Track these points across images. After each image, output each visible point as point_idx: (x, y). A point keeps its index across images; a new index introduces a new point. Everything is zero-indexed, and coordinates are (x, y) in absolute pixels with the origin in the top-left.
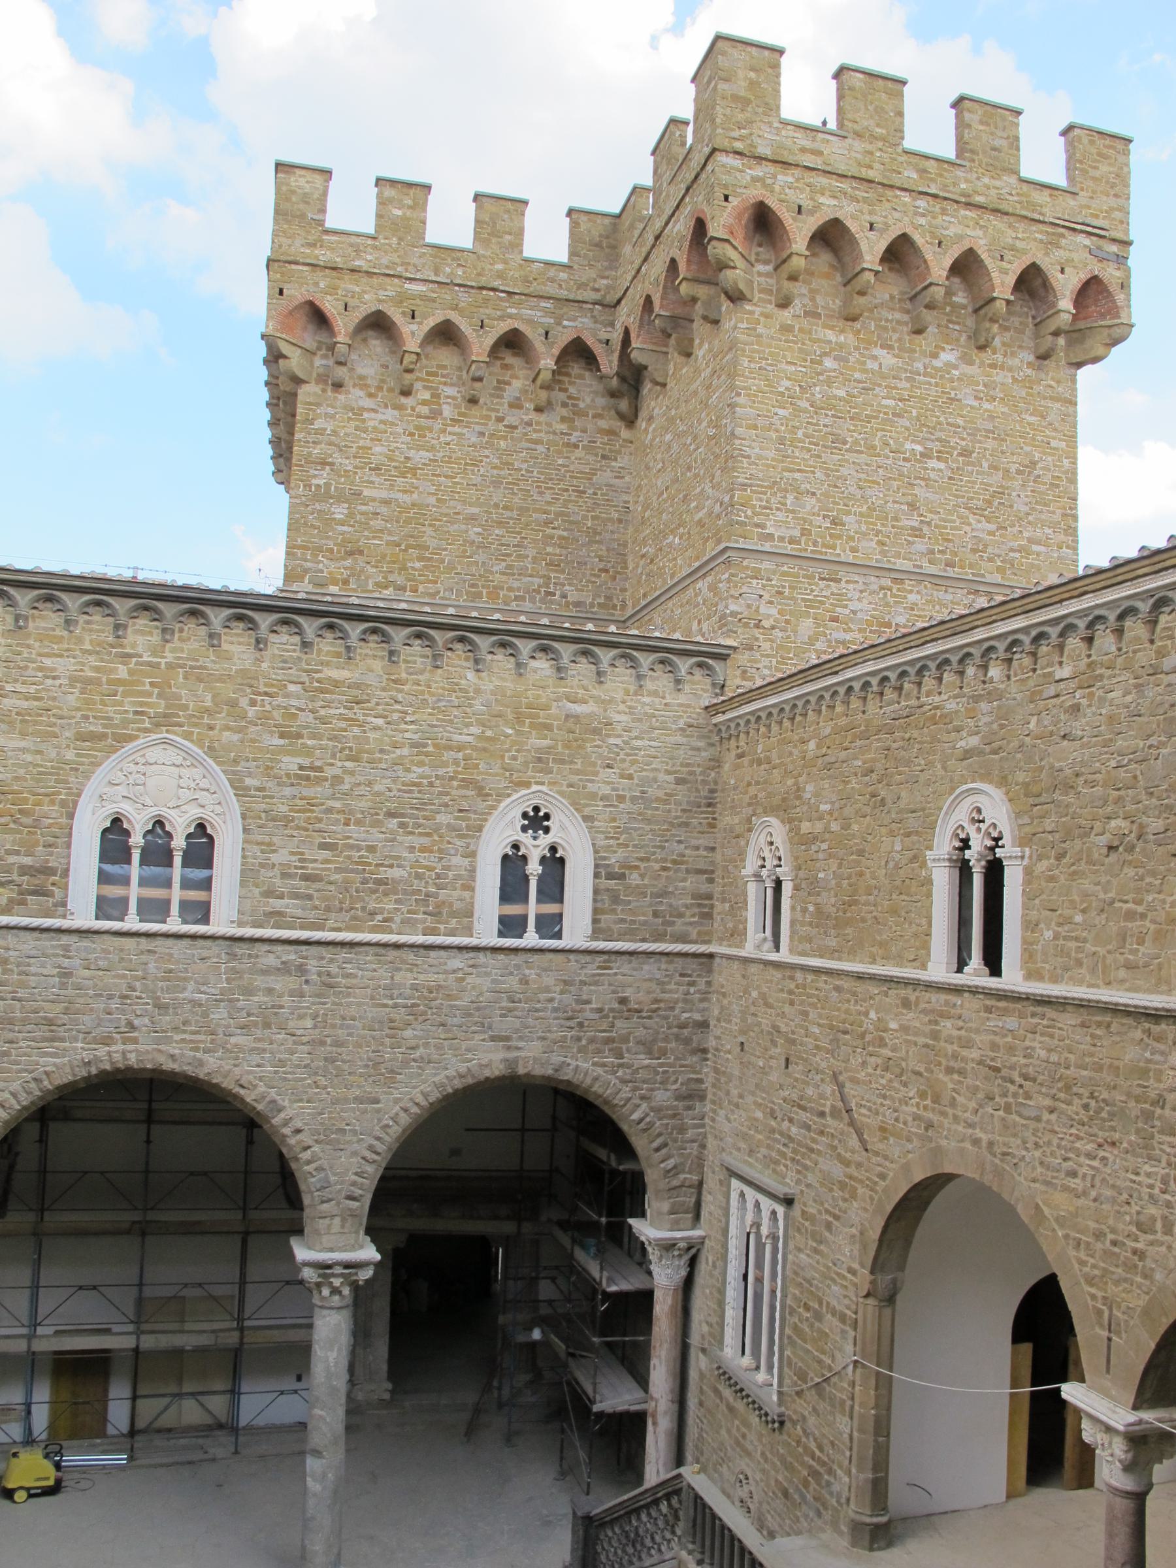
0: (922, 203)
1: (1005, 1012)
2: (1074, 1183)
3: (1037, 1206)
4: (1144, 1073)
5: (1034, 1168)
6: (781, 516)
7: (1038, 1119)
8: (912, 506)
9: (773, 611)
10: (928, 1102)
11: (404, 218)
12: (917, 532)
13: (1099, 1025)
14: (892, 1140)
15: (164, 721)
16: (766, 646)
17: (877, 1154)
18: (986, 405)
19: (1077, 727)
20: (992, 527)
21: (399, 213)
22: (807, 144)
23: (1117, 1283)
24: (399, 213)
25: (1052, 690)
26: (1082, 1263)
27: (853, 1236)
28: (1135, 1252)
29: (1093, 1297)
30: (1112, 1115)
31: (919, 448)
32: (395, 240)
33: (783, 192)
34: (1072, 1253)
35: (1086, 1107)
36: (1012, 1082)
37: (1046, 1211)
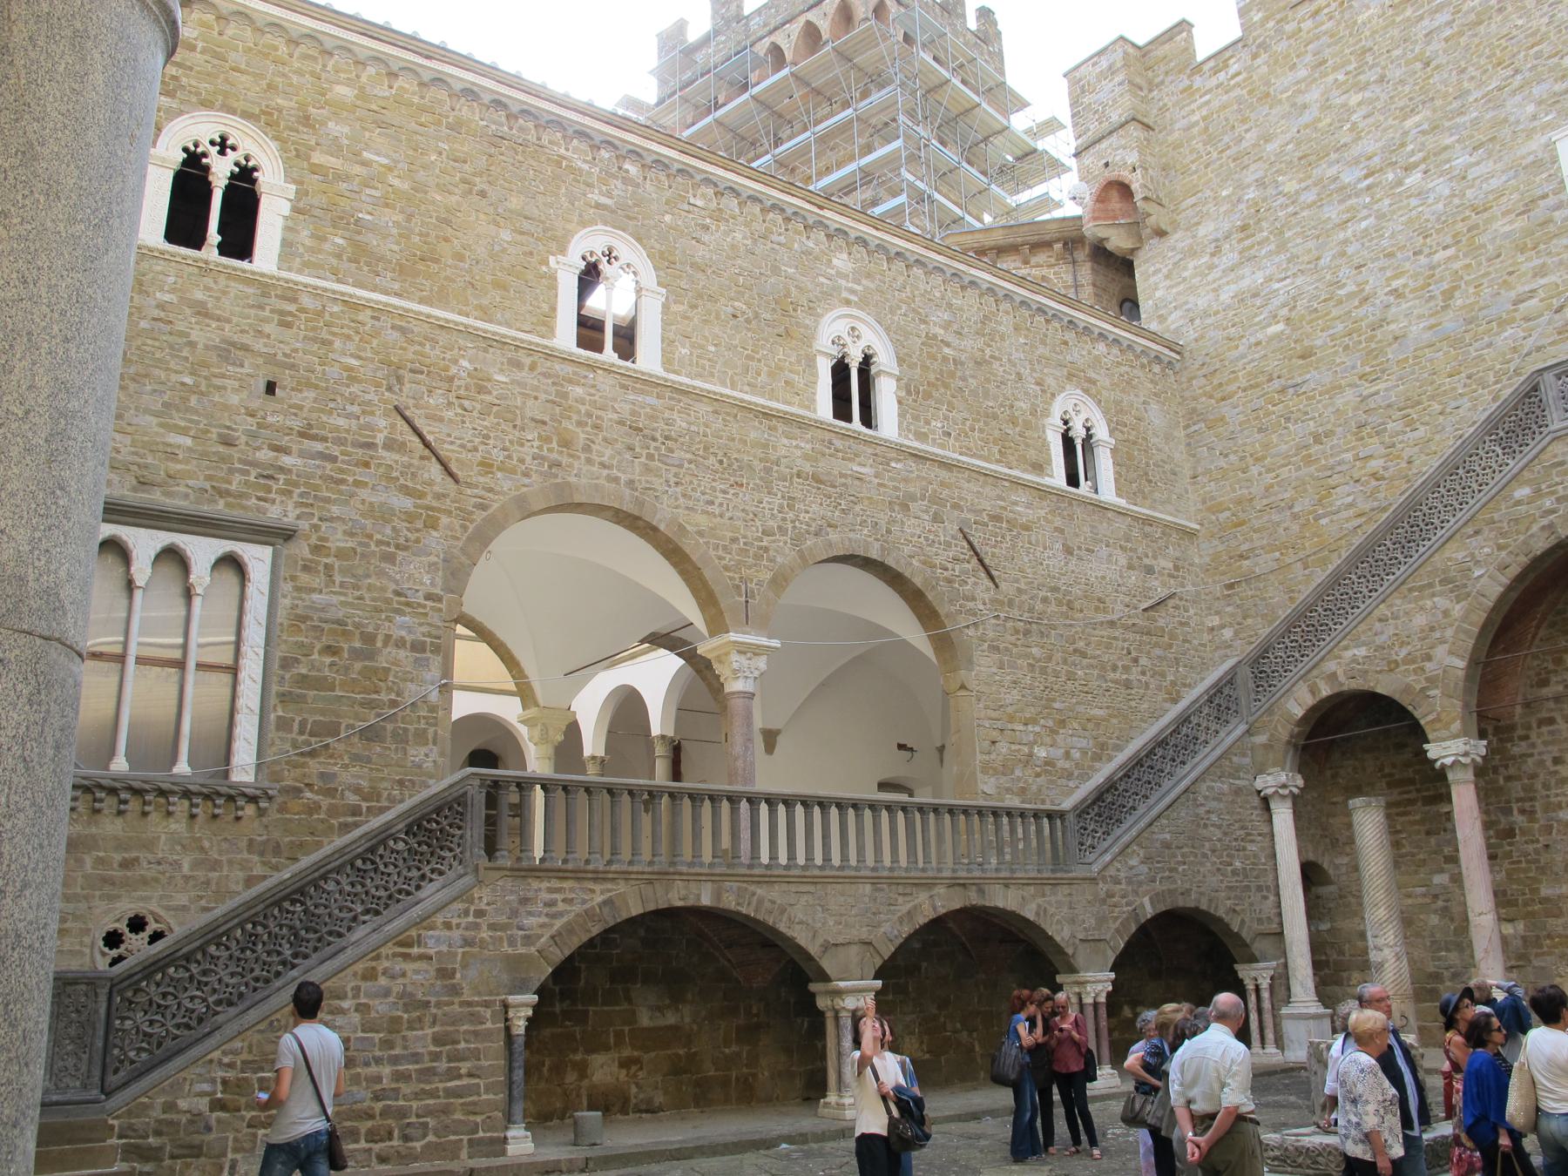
1: (642, 392)
2: (710, 508)
3: (680, 525)
4: (766, 446)
5: (677, 499)
7: (681, 466)
10: (554, 445)
13: (728, 414)
14: (499, 475)
17: (470, 486)
19: (706, 238)
23: (750, 568)
25: (686, 207)
26: (720, 558)
27: (435, 564)
28: (760, 548)
29: (731, 578)
30: (741, 468)
34: (712, 553)
35: (721, 462)
36: (654, 439)
37: (689, 528)
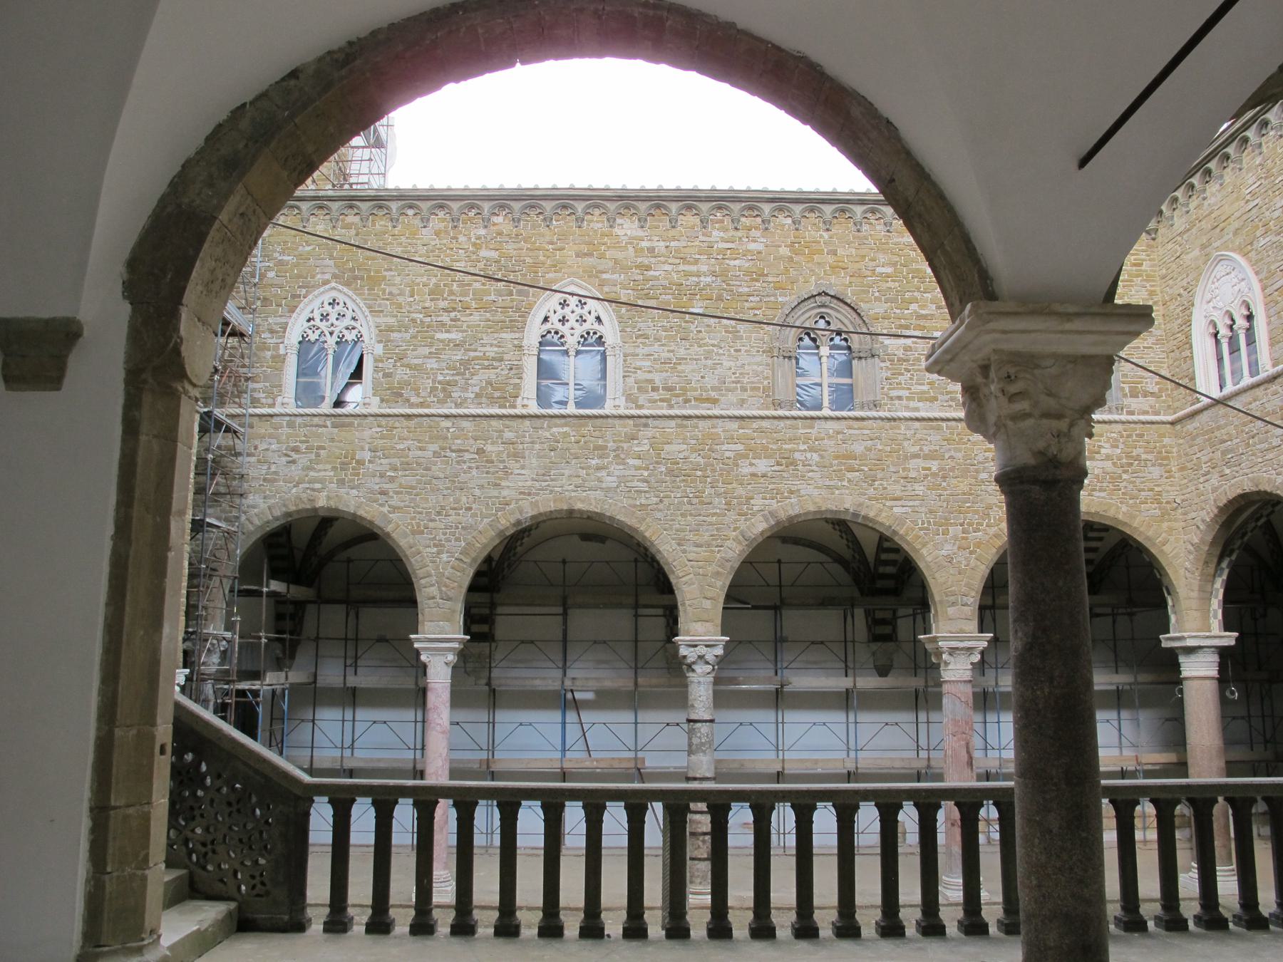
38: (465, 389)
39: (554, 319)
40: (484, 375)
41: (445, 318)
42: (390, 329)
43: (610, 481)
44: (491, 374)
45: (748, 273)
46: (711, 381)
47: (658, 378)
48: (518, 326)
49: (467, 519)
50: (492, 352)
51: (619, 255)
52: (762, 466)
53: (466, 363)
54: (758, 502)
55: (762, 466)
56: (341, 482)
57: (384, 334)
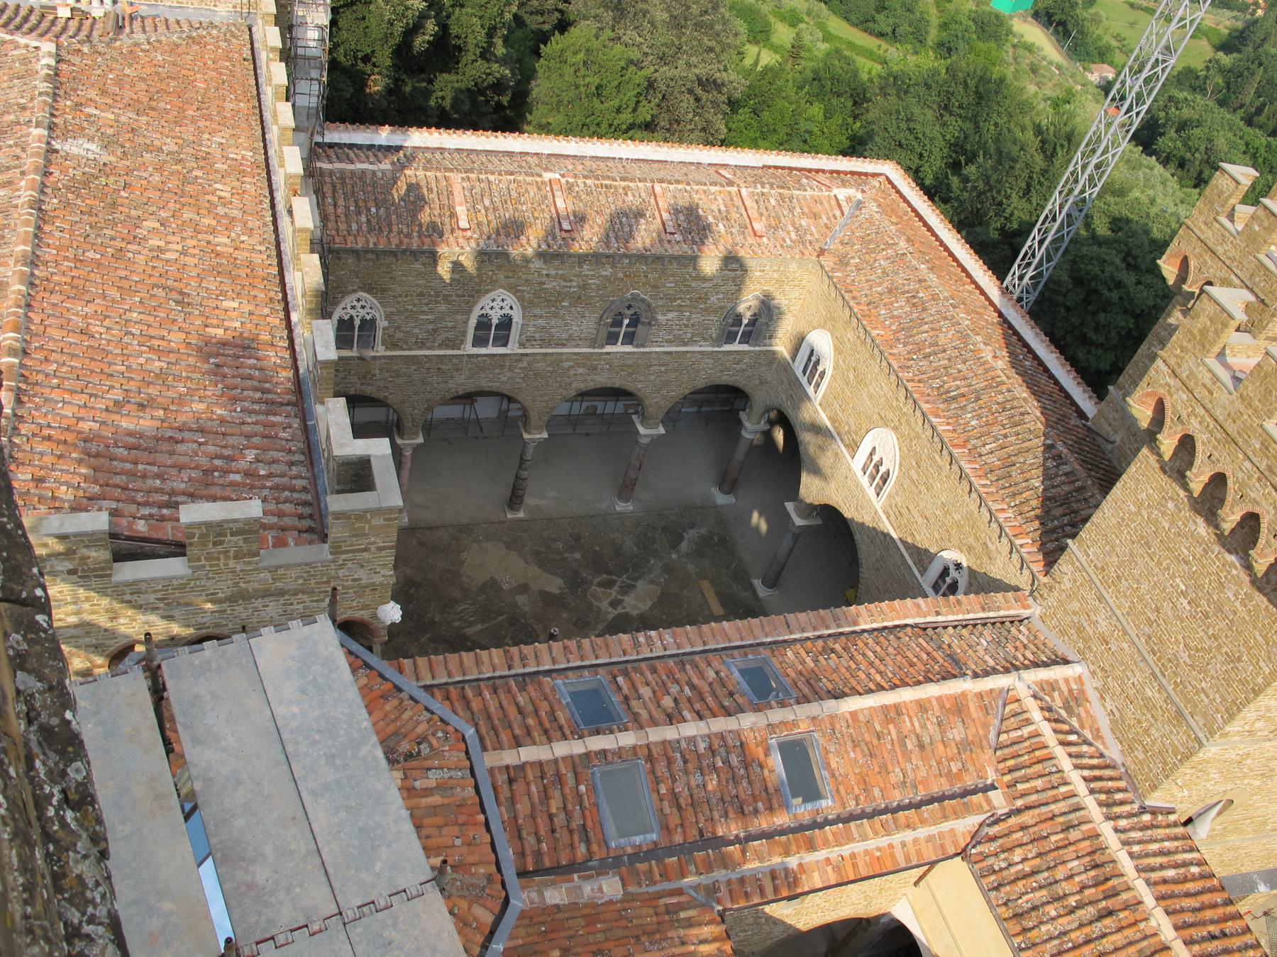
0: (1247, 464)
6: (1099, 551)
8: (1157, 610)
9: (1069, 585)
11: (1257, 233)
12: (1150, 623)
15: (895, 429)
16: (1056, 593)
18: (1237, 604)
20: (1188, 661)
21: (1257, 228)
22: (1208, 383)
24: (1257, 228)
31: (1183, 587)
32: (1243, 245)
33: (1177, 402)
38: (434, 341)
39: (487, 308)
40: (444, 335)
41: (425, 308)
42: (392, 313)
43: (504, 379)
44: (449, 335)
45: (598, 286)
46: (564, 336)
47: (537, 336)
48: (468, 312)
49: (429, 396)
50: (450, 324)
51: (530, 277)
52: (581, 370)
53: (435, 330)
54: (574, 385)
55: (581, 370)
56: (362, 384)
57: (388, 317)
